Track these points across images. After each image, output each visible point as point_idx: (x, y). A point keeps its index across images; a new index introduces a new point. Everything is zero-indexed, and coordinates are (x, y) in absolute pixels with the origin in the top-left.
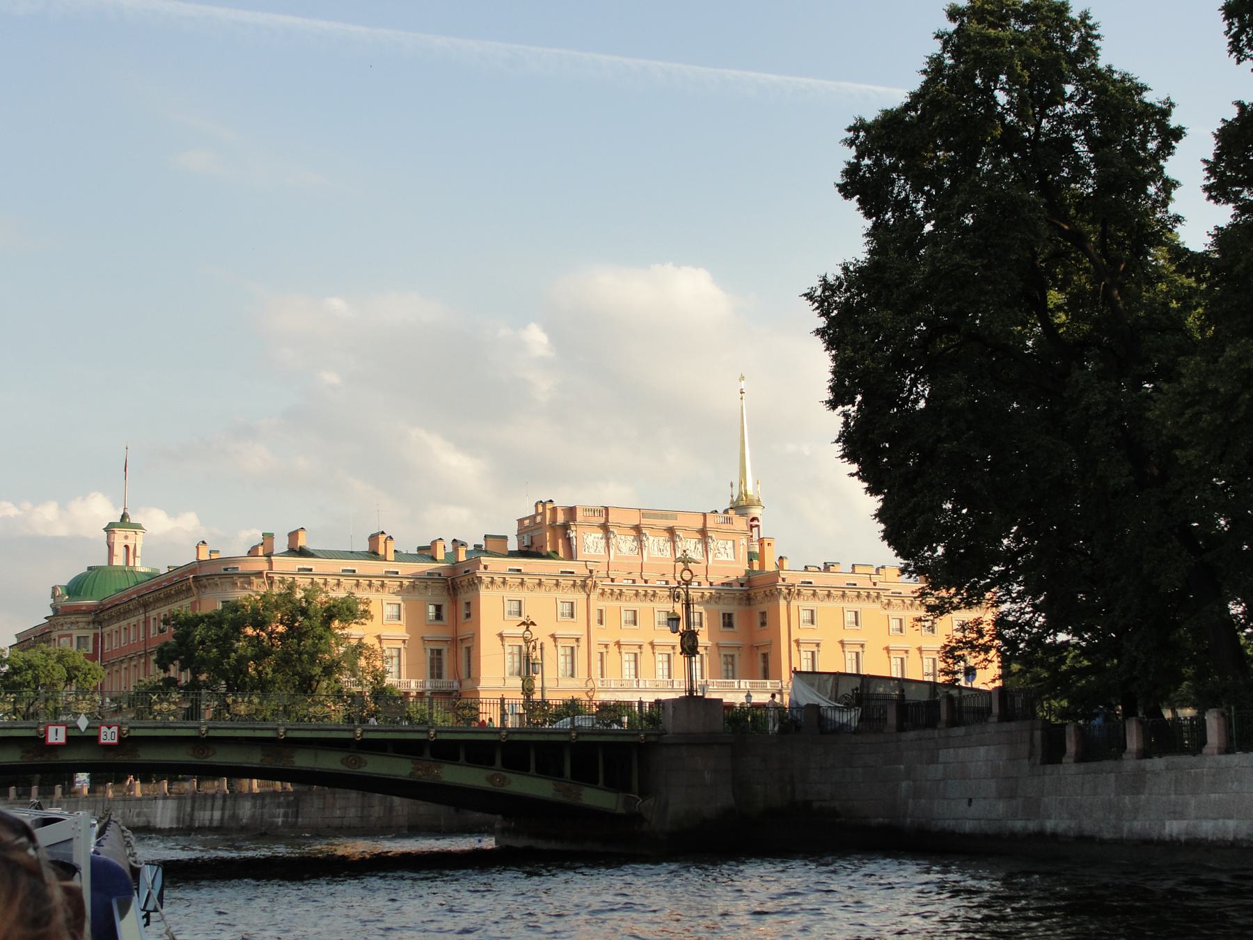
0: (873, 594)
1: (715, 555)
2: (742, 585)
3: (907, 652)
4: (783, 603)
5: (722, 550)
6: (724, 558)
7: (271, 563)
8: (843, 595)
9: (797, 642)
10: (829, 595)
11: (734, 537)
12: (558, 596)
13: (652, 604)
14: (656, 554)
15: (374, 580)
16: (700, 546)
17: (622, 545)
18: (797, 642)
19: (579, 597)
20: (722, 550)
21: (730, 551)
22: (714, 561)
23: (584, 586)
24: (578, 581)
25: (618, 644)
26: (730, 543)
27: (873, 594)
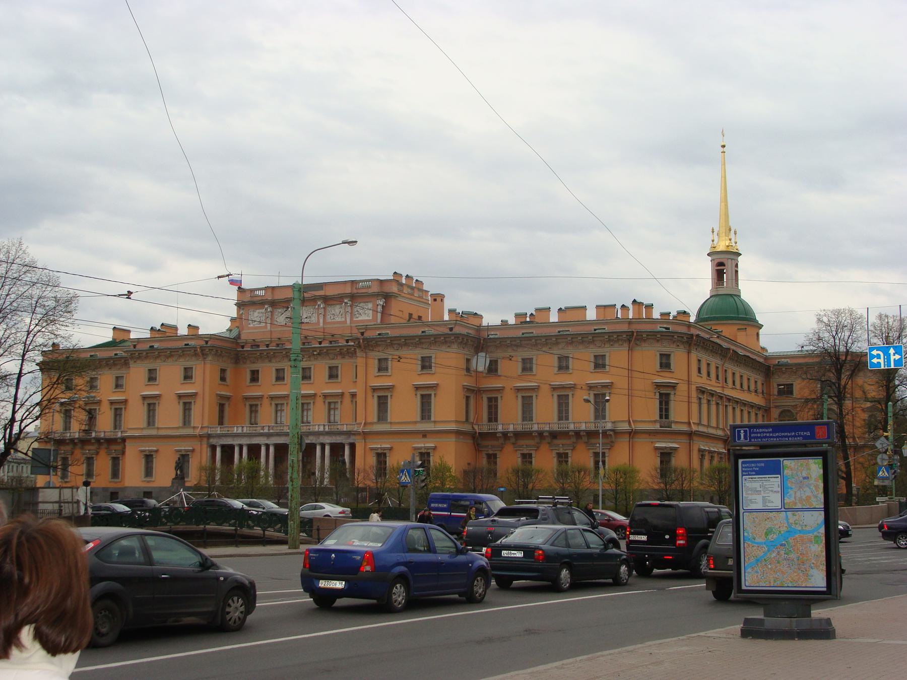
5: (361, 311)
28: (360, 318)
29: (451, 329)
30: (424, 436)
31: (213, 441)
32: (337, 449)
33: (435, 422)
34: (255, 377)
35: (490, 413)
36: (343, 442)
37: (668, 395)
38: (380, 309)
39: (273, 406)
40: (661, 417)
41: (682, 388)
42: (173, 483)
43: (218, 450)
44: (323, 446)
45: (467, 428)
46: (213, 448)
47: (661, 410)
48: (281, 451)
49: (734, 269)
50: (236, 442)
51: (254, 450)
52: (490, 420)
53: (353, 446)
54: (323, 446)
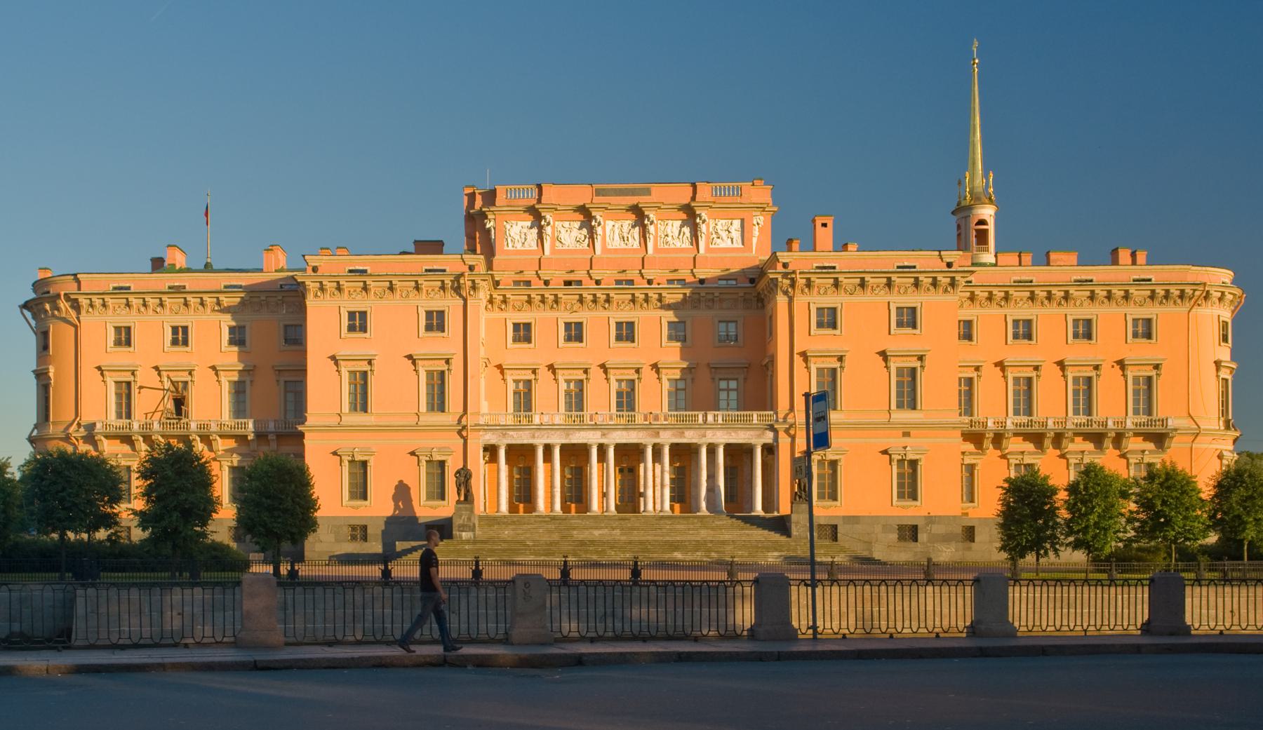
0: (944, 280)
1: (710, 241)
2: (752, 281)
3: (1036, 368)
4: (781, 300)
5: (724, 234)
6: (728, 244)
7: (79, 282)
8: (889, 284)
9: (804, 355)
10: (863, 284)
11: (744, 214)
12: (419, 303)
13: (606, 314)
14: (616, 243)
15: (205, 297)
16: (686, 230)
17: (564, 236)
18: (804, 355)
19: (450, 305)
20: (724, 234)
21: (736, 235)
22: (708, 249)
23: (457, 289)
24: (448, 282)
25: (551, 368)
26: (737, 223)
27: (944, 280)
28: (722, 245)
30: (907, 434)
31: (491, 438)
32: (738, 455)
34: (523, 333)
36: (753, 441)
42: (458, 510)
43: (502, 454)
44: (712, 450)
46: (491, 451)
48: (629, 456)
50: (540, 441)
51: (575, 456)
53: (769, 450)
54: (712, 450)
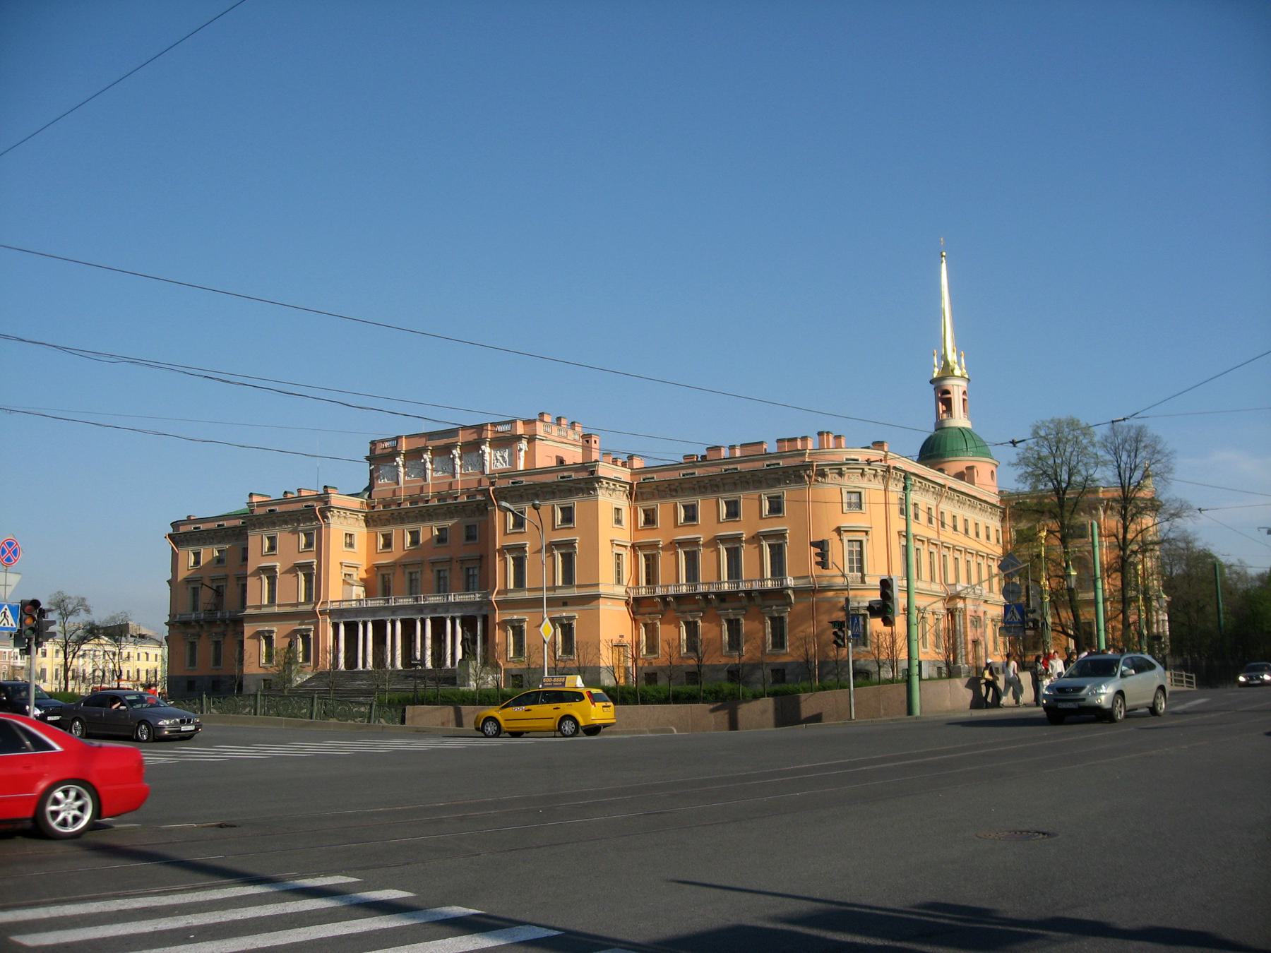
28: (500, 467)
29: (592, 473)
30: (565, 604)
33: (579, 586)
35: (648, 574)
36: (475, 613)
37: (861, 542)
38: (522, 454)
39: (407, 576)
40: (851, 570)
41: (878, 536)
45: (620, 590)
46: (336, 627)
47: (851, 561)
49: (961, 397)
52: (648, 582)
